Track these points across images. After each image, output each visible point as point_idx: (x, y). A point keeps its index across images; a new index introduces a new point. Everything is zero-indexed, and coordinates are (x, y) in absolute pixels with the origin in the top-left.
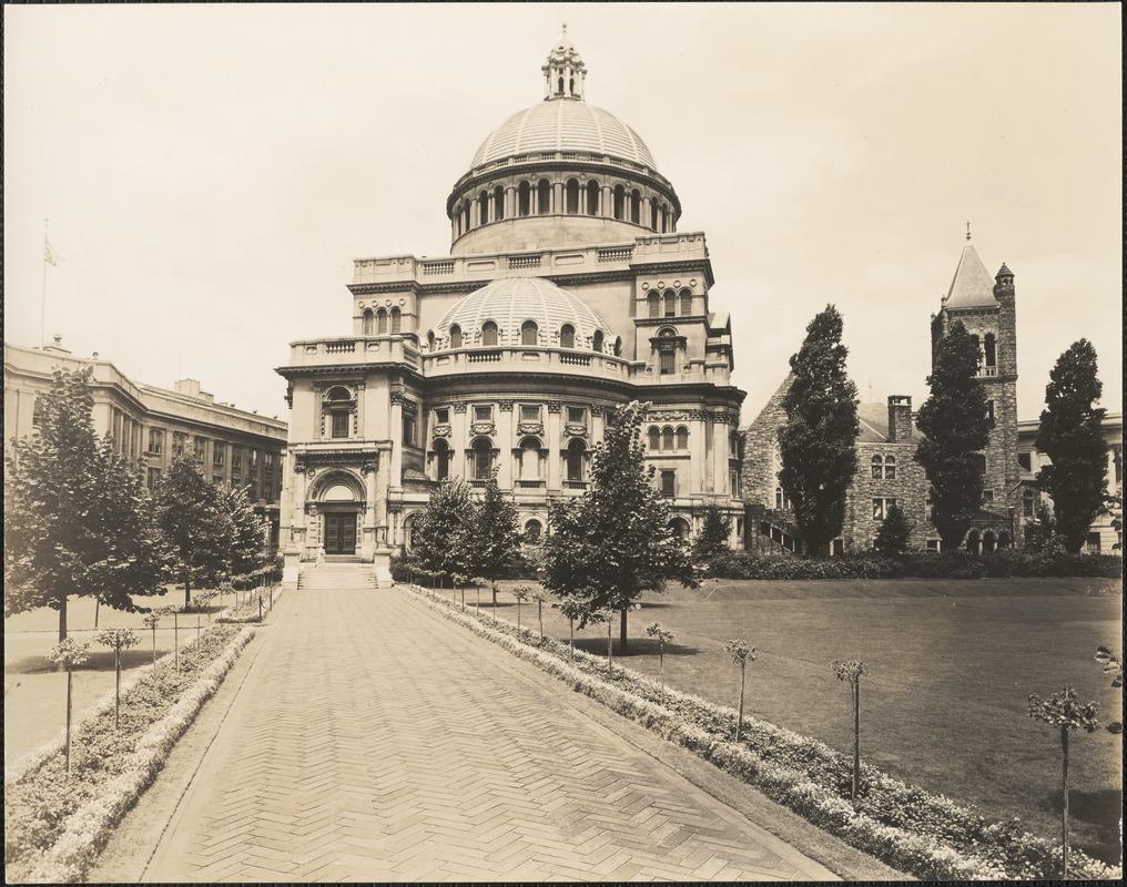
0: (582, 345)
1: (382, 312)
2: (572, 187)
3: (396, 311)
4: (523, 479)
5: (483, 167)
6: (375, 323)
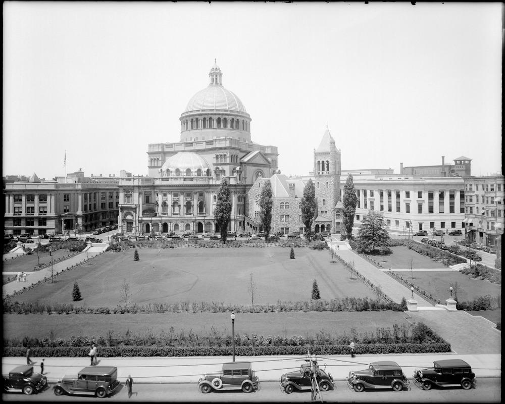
1: (155, 159)
2: (205, 119)
3: (158, 159)
6: (153, 163)
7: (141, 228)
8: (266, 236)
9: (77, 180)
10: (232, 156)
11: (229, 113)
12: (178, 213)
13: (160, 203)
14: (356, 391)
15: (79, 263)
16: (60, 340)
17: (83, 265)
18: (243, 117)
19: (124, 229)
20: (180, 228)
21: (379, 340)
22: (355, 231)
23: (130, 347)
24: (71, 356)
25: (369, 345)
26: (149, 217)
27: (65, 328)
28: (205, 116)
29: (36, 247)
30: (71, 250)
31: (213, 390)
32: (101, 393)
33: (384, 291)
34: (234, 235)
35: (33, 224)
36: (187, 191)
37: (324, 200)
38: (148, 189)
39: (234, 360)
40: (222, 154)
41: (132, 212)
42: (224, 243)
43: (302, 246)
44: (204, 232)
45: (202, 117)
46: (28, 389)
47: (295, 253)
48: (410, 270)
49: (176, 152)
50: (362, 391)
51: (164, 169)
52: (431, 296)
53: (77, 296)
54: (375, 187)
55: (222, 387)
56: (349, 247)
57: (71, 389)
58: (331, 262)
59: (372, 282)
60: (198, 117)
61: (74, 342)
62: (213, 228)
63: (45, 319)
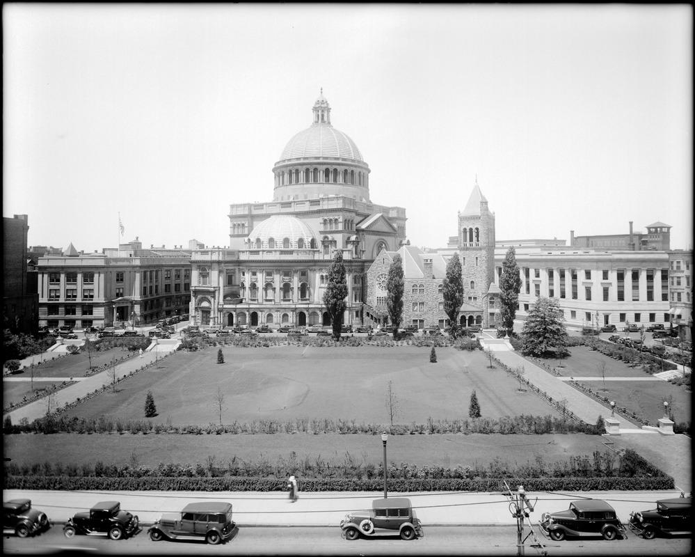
0: (294, 247)
1: (239, 225)
2: (307, 170)
3: (243, 225)
4: (268, 298)
5: (284, 161)
6: (236, 229)
7: (222, 319)
8: (395, 332)
9: (132, 253)
10: (346, 220)
11: (340, 161)
12: (271, 298)
13: (247, 285)
14: (553, 539)
15: (144, 366)
16: (145, 468)
17: (150, 370)
18: (359, 167)
19: (198, 321)
20: (275, 320)
21: (575, 473)
22: (519, 326)
23: (239, 478)
24: (162, 490)
25: (563, 479)
26: (233, 304)
27: (147, 453)
28: (308, 166)
29: (83, 344)
30: (130, 349)
31: (361, 536)
32: (213, 538)
33: (570, 409)
34: (349, 329)
35: (74, 313)
36: (285, 268)
37: (472, 282)
38: (232, 266)
39: (386, 497)
40: (331, 218)
41: (209, 297)
42: (338, 340)
43: (444, 345)
44: (307, 325)
45: (305, 167)
46: (116, 532)
47: (437, 355)
48: (602, 379)
49: (268, 216)
50: (562, 540)
51: (253, 239)
52: (634, 414)
53: (151, 411)
54: (543, 264)
55: (373, 532)
56: (511, 347)
57: (172, 533)
58: (488, 367)
59: (549, 395)
60: (299, 167)
61: (164, 470)
62: (320, 320)
63: (116, 441)
